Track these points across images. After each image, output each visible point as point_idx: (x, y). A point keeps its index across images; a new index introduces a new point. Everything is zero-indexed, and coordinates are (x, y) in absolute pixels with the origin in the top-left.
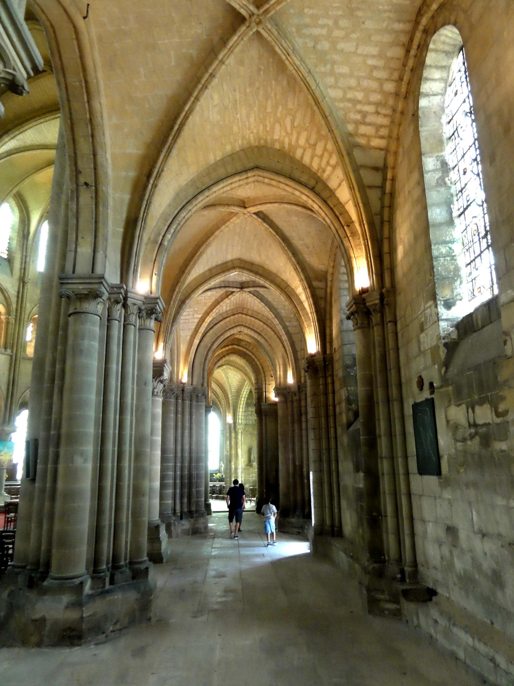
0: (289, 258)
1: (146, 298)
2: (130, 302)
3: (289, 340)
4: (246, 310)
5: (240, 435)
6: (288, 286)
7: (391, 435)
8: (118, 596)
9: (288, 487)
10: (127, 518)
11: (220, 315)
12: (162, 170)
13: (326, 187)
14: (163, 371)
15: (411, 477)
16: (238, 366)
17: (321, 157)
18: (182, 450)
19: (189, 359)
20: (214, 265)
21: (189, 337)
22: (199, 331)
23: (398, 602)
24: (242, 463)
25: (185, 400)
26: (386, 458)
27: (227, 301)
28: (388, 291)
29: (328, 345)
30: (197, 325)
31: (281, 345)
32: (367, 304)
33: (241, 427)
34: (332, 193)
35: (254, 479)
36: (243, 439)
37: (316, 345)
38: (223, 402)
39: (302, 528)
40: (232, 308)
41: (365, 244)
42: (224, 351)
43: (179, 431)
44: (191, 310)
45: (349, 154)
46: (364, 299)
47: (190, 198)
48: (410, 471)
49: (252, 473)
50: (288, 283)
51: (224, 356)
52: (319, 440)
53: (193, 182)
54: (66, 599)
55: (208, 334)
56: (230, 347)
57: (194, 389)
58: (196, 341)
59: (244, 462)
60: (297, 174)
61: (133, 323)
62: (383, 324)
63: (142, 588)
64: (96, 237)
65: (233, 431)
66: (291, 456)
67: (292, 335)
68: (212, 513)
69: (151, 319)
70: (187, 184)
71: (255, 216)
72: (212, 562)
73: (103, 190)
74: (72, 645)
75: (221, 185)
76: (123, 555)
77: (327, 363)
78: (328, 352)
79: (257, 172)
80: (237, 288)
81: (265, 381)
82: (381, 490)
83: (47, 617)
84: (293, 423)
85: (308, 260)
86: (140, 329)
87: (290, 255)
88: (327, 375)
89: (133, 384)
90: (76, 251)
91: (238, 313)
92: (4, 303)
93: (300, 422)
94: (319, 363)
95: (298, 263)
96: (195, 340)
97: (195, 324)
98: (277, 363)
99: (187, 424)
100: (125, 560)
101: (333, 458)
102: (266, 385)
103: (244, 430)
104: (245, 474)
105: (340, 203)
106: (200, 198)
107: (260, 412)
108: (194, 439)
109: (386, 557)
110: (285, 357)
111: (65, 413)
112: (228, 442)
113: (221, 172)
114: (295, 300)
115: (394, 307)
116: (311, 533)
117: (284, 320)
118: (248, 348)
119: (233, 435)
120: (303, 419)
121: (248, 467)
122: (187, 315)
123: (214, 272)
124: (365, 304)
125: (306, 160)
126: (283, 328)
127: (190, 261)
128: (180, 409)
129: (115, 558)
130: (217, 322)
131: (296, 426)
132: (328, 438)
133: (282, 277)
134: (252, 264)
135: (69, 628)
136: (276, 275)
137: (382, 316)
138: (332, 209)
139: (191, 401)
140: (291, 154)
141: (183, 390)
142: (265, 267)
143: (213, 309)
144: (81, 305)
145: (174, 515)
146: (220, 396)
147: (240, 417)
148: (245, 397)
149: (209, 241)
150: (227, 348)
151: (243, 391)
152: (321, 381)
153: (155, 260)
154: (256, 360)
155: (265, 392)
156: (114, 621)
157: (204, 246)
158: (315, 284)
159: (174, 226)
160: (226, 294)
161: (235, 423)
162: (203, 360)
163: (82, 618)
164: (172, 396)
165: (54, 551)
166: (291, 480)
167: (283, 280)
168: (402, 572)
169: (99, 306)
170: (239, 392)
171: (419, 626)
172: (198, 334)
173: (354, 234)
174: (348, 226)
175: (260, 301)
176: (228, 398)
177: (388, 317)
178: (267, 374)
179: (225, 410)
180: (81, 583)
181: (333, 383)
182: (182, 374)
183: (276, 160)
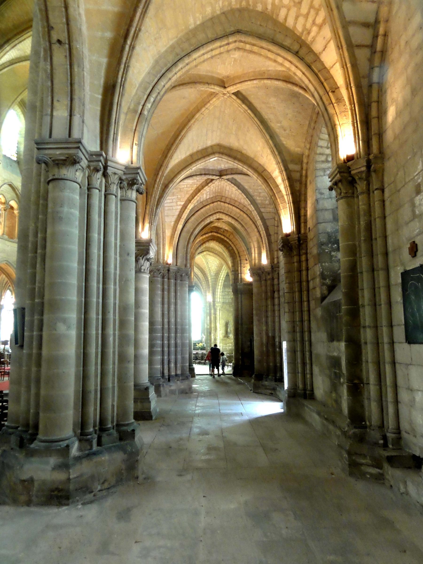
0: (267, 141)
1: (127, 168)
2: (110, 171)
3: (263, 225)
4: (224, 198)
6: (265, 170)
7: (375, 305)
8: (105, 457)
9: (261, 353)
10: (113, 383)
11: (200, 203)
12: (140, 30)
13: (311, 51)
14: (149, 250)
15: (397, 346)
16: (216, 252)
17: (306, 16)
18: (169, 322)
19: (174, 243)
20: (195, 150)
21: (173, 223)
22: (182, 218)
23: (380, 467)
25: (170, 279)
26: (369, 327)
27: (207, 189)
28: (376, 157)
29: (302, 225)
30: (180, 212)
31: (256, 230)
32: (353, 172)
33: (220, 304)
34: (317, 58)
35: (230, 348)
36: (221, 315)
37: (291, 225)
38: (204, 283)
39: (274, 389)
40: (212, 196)
41: (351, 109)
42: (204, 238)
43: (166, 306)
44: (174, 197)
45: (338, 8)
46: (349, 168)
47: (169, 65)
48: (395, 340)
49: (229, 343)
50: (265, 167)
51: (204, 243)
52: (292, 312)
53: (173, 48)
54: (53, 461)
55: (190, 221)
56: (210, 234)
57: (179, 270)
58: (180, 227)
59: (222, 334)
60: (279, 38)
61: (114, 192)
62: (368, 192)
63: (129, 449)
64: (72, 100)
65: (213, 308)
66: (264, 328)
67: (266, 220)
68: (196, 376)
69: (133, 190)
70: (166, 51)
71: (233, 97)
72: (196, 419)
73: (77, 48)
74: (60, 504)
75: (202, 51)
76: (110, 418)
77: (301, 242)
78: (302, 231)
79: (238, 37)
80: (216, 175)
81: (241, 264)
82: (364, 359)
83: (35, 478)
84: (267, 299)
85: (285, 143)
86: (121, 200)
87: (268, 137)
88: (301, 254)
89: (116, 254)
90: (52, 115)
91: (217, 201)
92: (16, 199)
93: (273, 298)
94: (294, 242)
95: (275, 146)
96: (179, 225)
97: (179, 210)
98: (252, 247)
99: (173, 300)
100: (112, 422)
101: (306, 329)
102: (242, 268)
103: (222, 307)
104: (223, 344)
105: (325, 68)
106: (180, 65)
107: (236, 291)
108: (179, 313)
109: (368, 423)
110: (260, 240)
111: (47, 281)
112: (208, 317)
113: (201, 37)
114: (271, 183)
115: (381, 173)
116: (284, 395)
117: (259, 206)
118: (225, 235)
119: (212, 311)
120: (276, 295)
122: (171, 202)
123: (195, 158)
124: (350, 172)
125: (290, 23)
126: (259, 214)
127: (172, 144)
128: (166, 287)
129: (102, 421)
130: (198, 209)
131: (269, 302)
132: (301, 312)
133: (259, 162)
134: (230, 149)
135: (57, 489)
136: (253, 160)
137: (368, 184)
138: (316, 75)
139: (175, 280)
140: (274, 17)
141: (169, 270)
142: (243, 152)
143: (195, 196)
144: (59, 172)
145: (163, 378)
146: (201, 279)
147: (218, 296)
148: (222, 280)
149: (190, 124)
150: (207, 235)
151: (221, 274)
152: (295, 259)
153: (135, 130)
154: (232, 245)
155: (241, 273)
156: (102, 481)
157: (185, 129)
158: (292, 166)
159: (154, 95)
160: (206, 182)
161: (214, 301)
162: (186, 244)
163: (69, 479)
164: (159, 276)
165: (41, 415)
166: (264, 349)
167: (260, 165)
168: (385, 438)
169: (78, 173)
170: (217, 274)
171: (407, 493)
172: (181, 220)
173: (339, 100)
174: (333, 92)
175: (237, 189)
176: (208, 280)
177: (375, 184)
178: (242, 258)
179: (206, 291)
180: (68, 446)
181: (307, 260)
182: (168, 256)
183: (259, 23)
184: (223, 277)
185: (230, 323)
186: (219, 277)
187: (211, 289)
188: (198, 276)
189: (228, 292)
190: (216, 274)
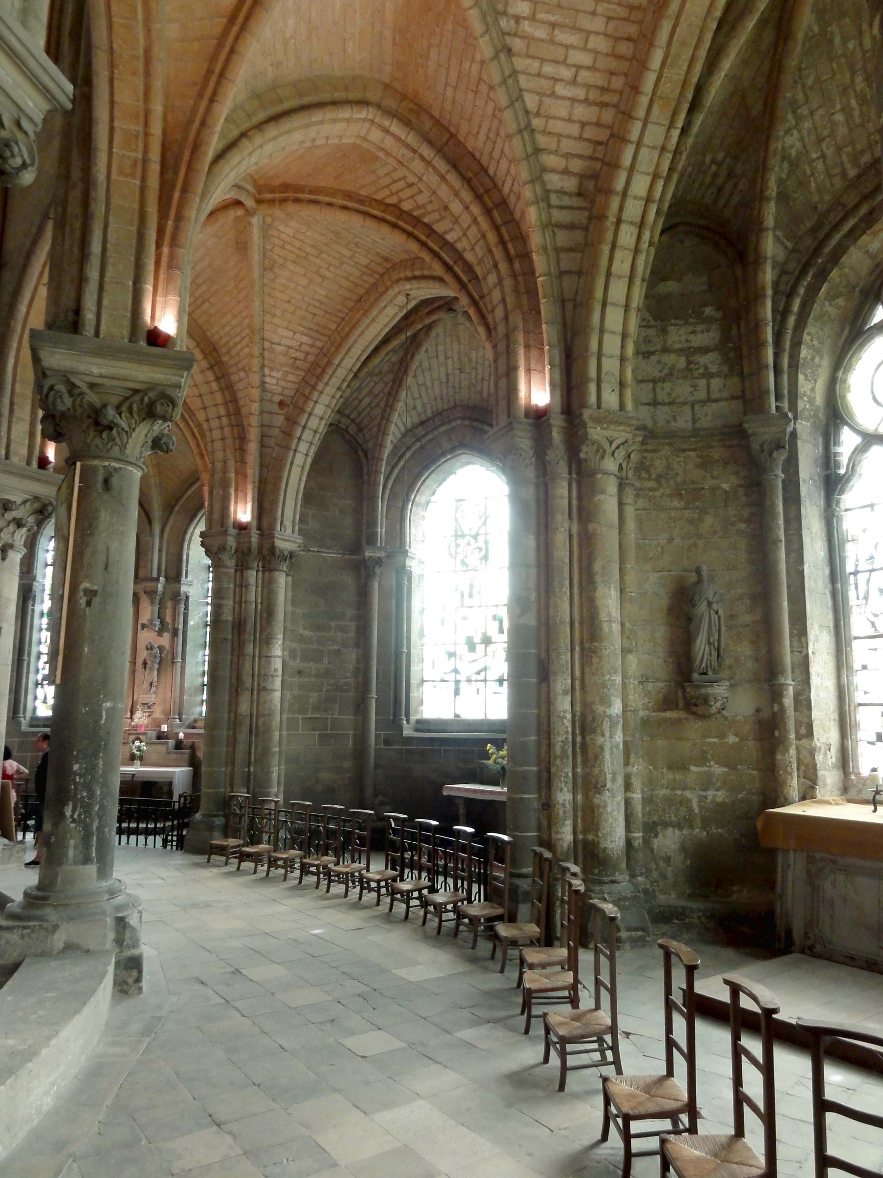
5: (612, 487)
24: (633, 683)
33: (620, 434)
35: (720, 796)
36: (631, 525)
49: (702, 760)
59: (644, 680)
103: (642, 467)
104: (652, 760)
119: (562, 491)
121: (668, 714)
147: (611, 365)
148: (642, 225)
151: (627, 159)
184: (648, 200)
185: (710, 591)
186: (609, 192)
187: (546, 307)
188: (459, 256)
189: (689, 352)
190: (590, 185)
